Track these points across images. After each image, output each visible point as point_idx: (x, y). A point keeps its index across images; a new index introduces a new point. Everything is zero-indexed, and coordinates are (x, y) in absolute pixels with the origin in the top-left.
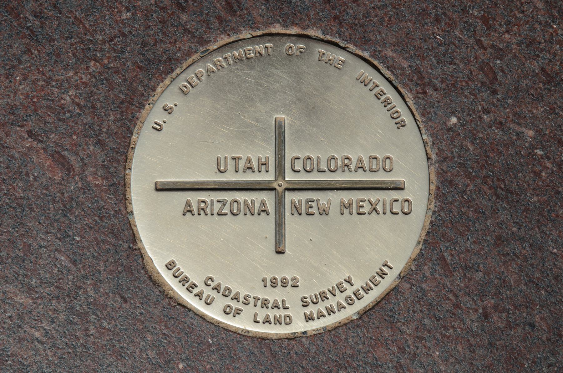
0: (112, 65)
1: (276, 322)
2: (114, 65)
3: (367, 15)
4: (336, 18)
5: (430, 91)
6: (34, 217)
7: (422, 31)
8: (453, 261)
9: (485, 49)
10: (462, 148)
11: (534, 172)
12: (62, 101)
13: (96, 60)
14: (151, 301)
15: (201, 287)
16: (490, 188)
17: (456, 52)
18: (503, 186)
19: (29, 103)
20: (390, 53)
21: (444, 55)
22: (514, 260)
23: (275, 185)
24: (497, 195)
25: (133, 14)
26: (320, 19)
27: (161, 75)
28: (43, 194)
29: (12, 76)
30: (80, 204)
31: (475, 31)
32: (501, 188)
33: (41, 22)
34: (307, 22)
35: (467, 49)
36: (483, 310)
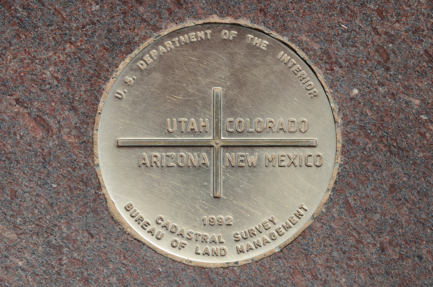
0: (84, 47)
1: (214, 254)
2: (85, 47)
3: (286, 8)
4: (261, 10)
5: (336, 68)
6: (20, 168)
7: (330, 21)
8: (356, 204)
9: (380, 35)
10: (362, 113)
11: (420, 133)
12: (44, 76)
13: (71, 43)
14: (113, 237)
15: (153, 226)
16: (385, 146)
17: (357, 38)
18: (395, 144)
19: (17, 77)
20: (304, 38)
21: (348, 39)
22: (405, 204)
23: (213, 143)
24: (391, 152)
25: (101, 7)
26: (249, 11)
27: (123, 55)
28: (27, 150)
29: (4, 55)
30: (57, 157)
31: (371, 21)
32: (393, 146)
33: (29, 14)
34: (239, 14)
35: (366, 35)
36: (380, 245)
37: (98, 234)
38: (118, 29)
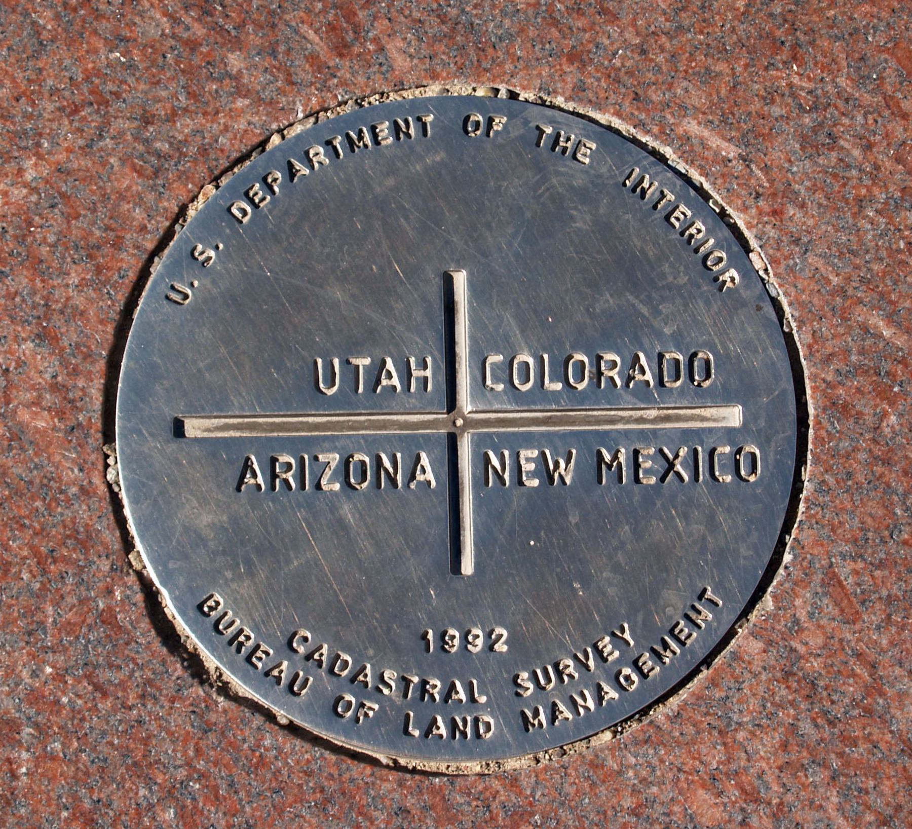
2: (80, 164)
8: (859, 585)
13: (40, 157)
17: (843, 125)
21: (815, 130)
31: (881, 78)
37: (122, 685)
38: (172, 117)
